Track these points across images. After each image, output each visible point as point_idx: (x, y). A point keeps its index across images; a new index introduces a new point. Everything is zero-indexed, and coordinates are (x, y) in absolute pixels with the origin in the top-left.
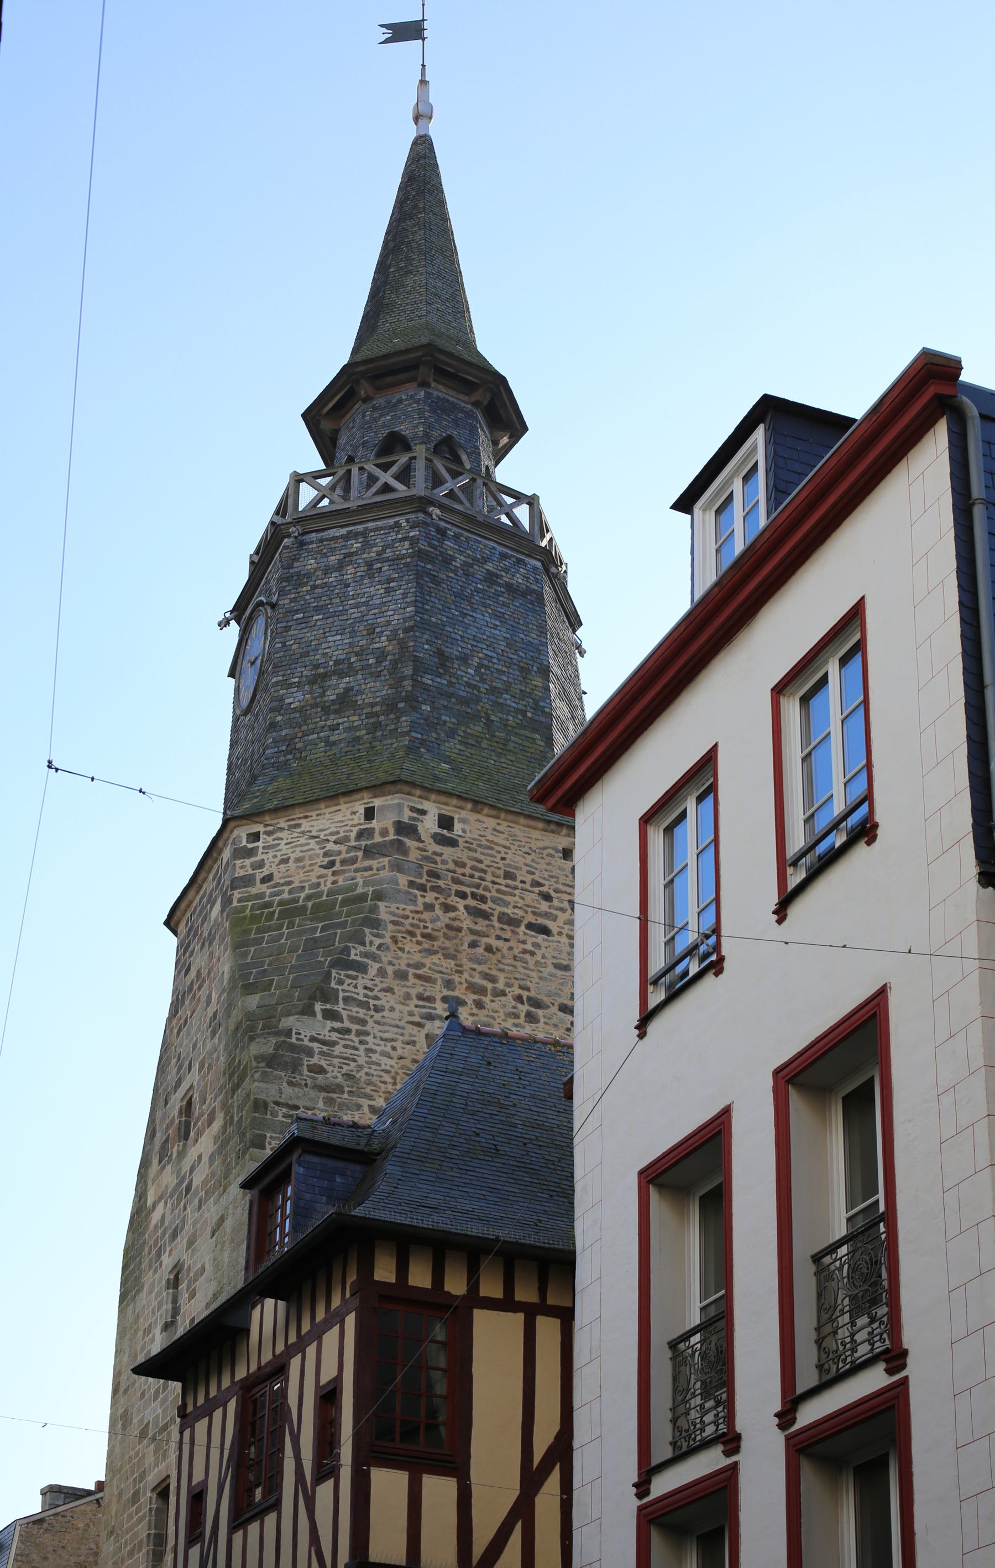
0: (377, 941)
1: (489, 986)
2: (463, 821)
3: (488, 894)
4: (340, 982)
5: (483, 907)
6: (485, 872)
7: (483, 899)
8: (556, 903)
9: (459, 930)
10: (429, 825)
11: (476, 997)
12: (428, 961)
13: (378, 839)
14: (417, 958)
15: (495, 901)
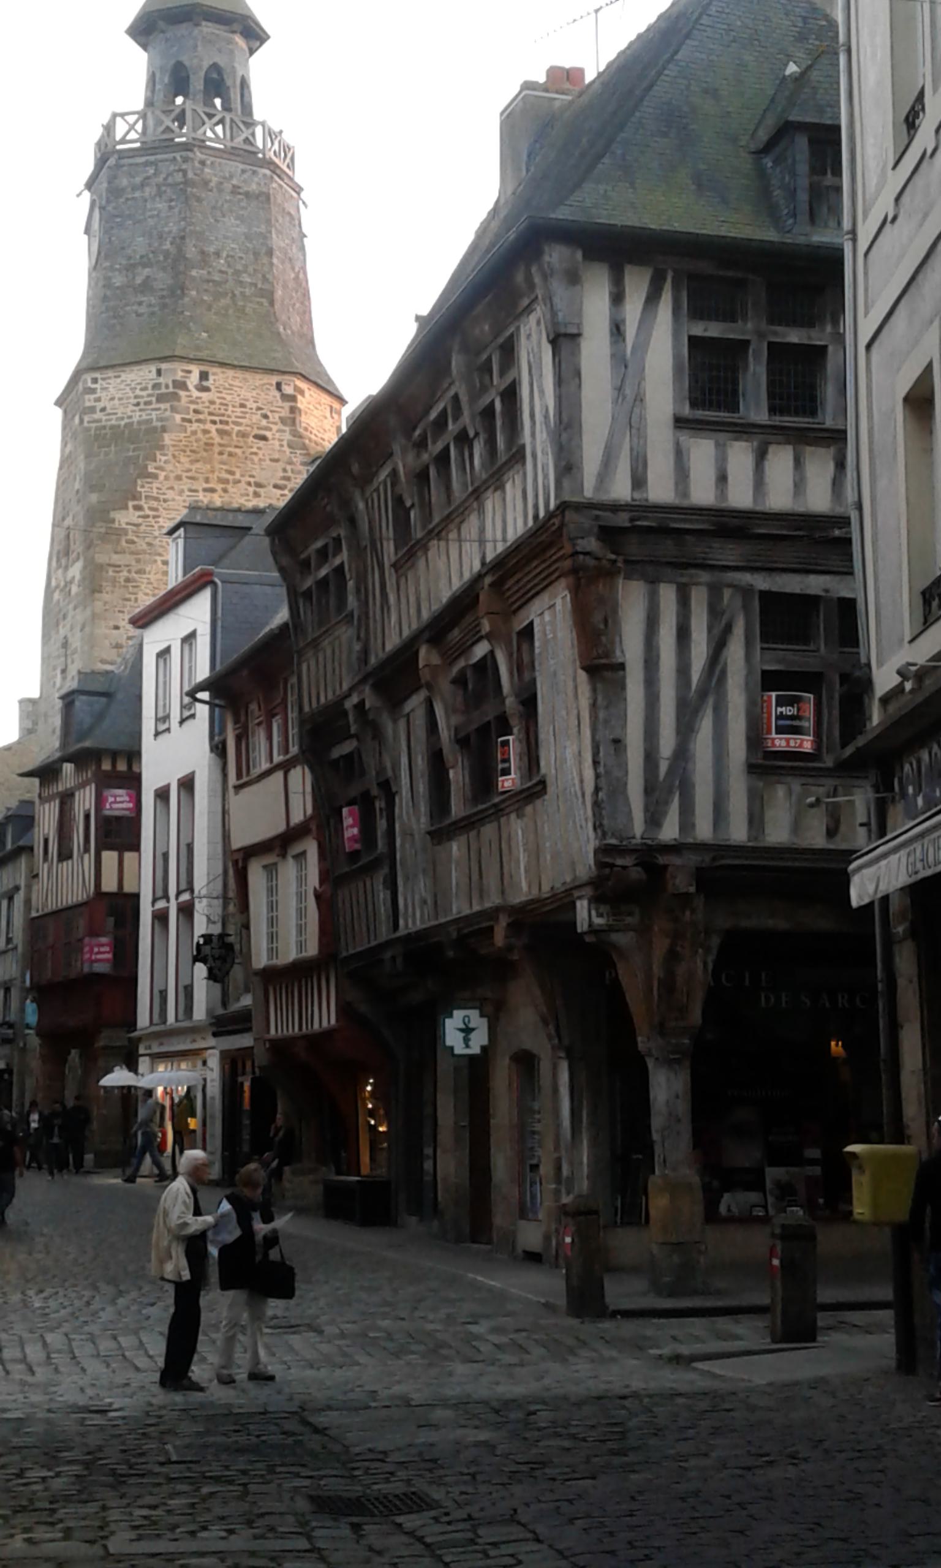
0: (164, 458)
1: (230, 477)
2: (214, 374)
3: (230, 420)
4: (143, 487)
5: (226, 428)
6: (226, 405)
7: (227, 423)
8: (271, 419)
9: (212, 445)
10: (194, 379)
11: (223, 486)
12: (194, 467)
13: (163, 390)
14: (187, 466)
15: (234, 423)
